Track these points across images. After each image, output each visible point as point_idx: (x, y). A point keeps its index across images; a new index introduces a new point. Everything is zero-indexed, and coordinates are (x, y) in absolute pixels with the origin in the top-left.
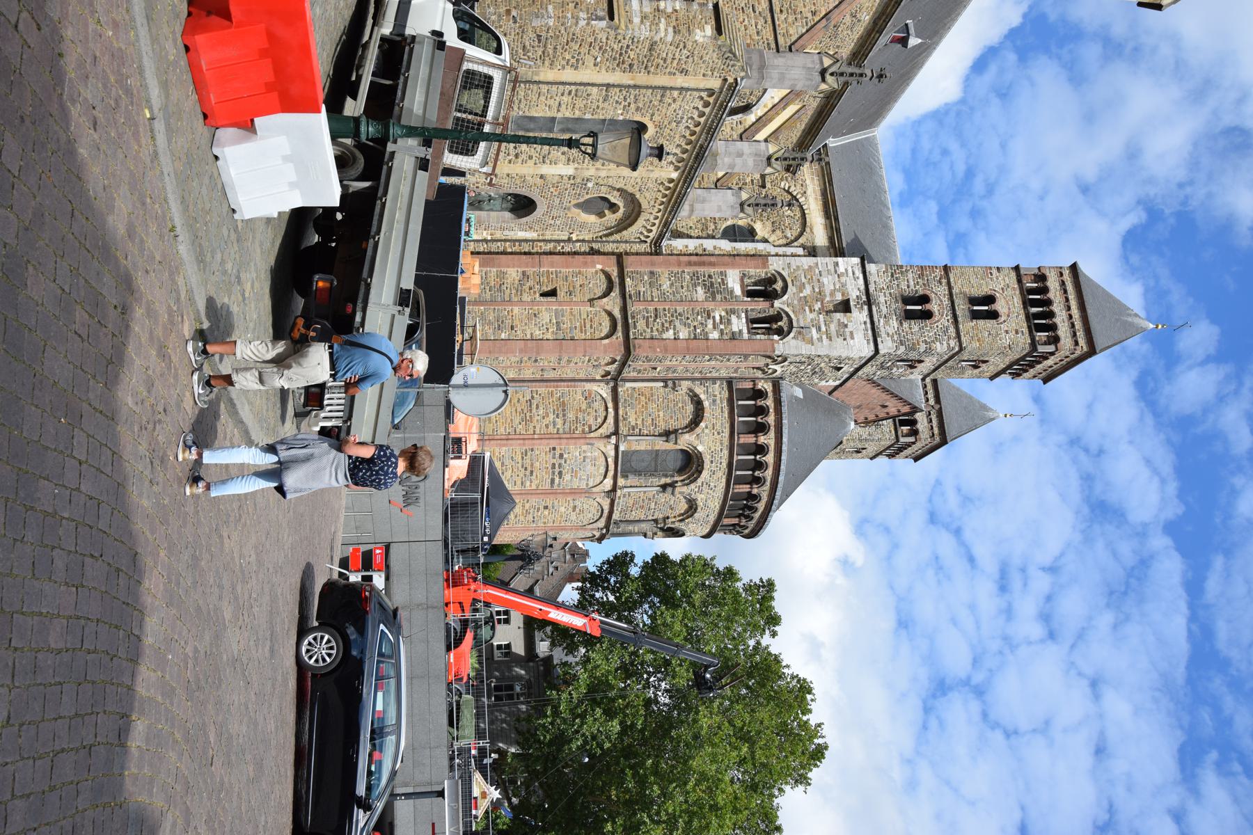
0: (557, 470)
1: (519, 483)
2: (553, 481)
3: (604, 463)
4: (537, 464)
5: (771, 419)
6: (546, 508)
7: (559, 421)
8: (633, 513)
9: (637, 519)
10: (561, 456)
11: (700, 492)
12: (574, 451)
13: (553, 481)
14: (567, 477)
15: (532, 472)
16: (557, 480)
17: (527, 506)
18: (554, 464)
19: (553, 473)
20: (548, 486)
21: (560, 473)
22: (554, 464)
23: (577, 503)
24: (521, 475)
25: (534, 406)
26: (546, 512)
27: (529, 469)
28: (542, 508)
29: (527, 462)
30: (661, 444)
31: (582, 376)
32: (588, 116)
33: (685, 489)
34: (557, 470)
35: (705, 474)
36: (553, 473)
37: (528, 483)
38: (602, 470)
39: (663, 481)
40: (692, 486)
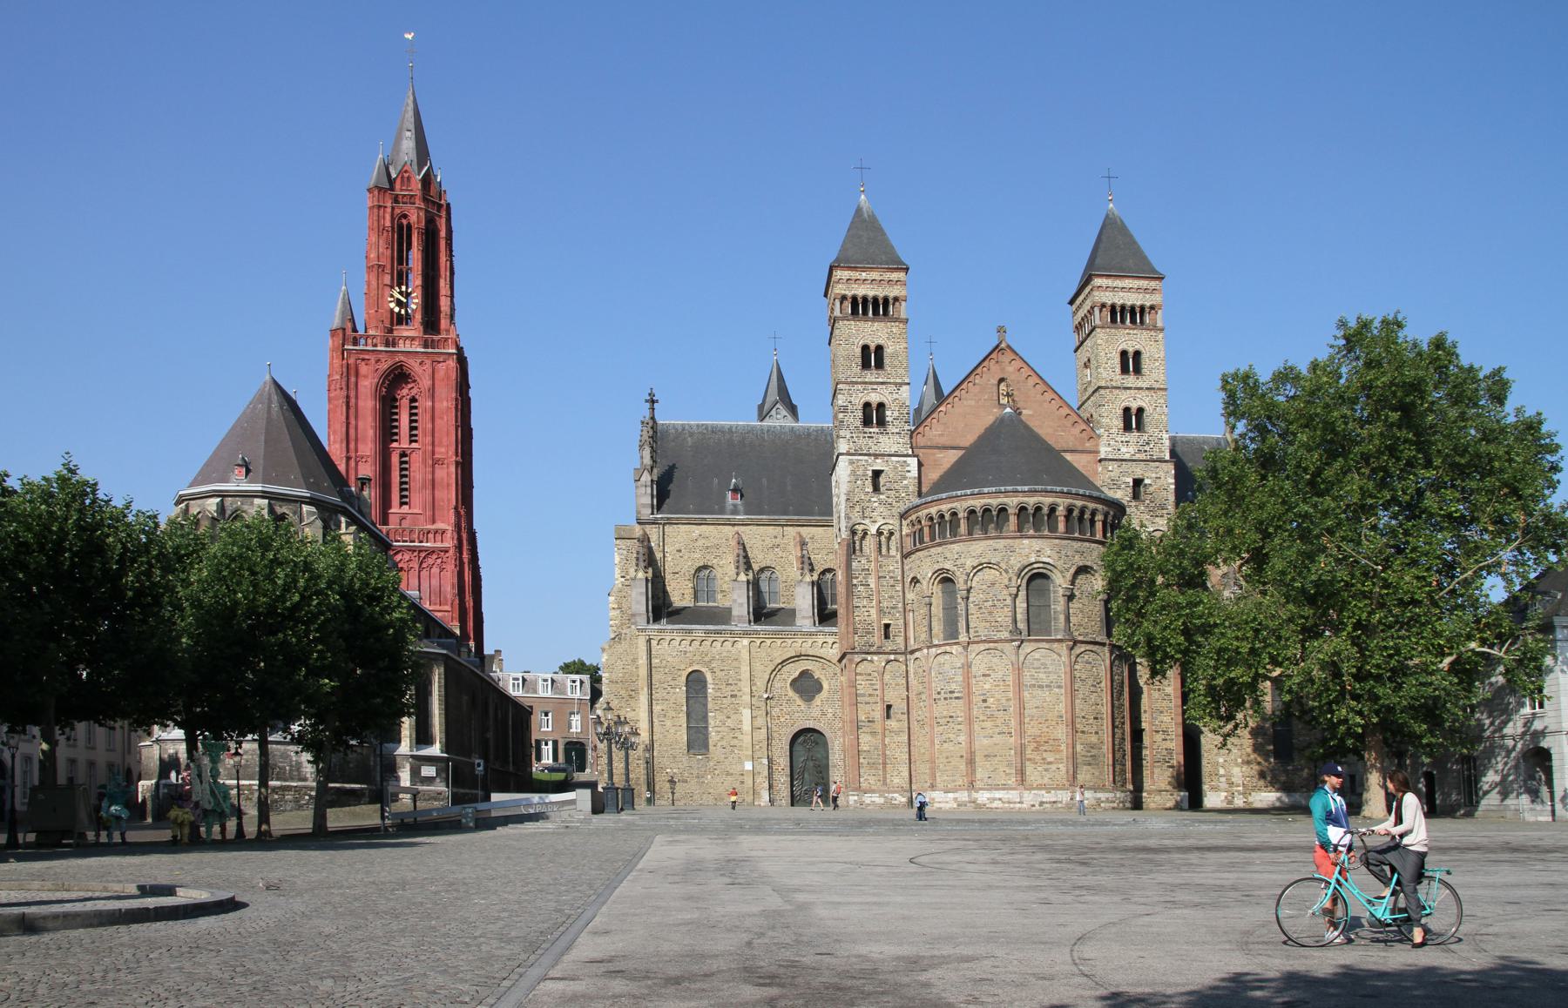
0: (948, 695)
1: (959, 727)
2: (957, 698)
3: (942, 656)
4: (945, 713)
5: (914, 517)
6: (985, 701)
7: (923, 697)
8: (999, 619)
9: (1010, 614)
10: (939, 693)
11: (963, 565)
12: (937, 685)
13: (957, 698)
14: (953, 687)
15: (951, 717)
16: (956, 695)
17: (982, 718)
18: (945, 699)
19: (951, 698)
20: (961, 701)
21: (951, 692)
22: (945, 699)
23: (980, 673)
24: (953, 725)
25: (919, 718)
26: (991, 700)
27: (948, 719)
28: (985, 705)
29: (943, 721)
30: (937, 610)
31: (904, 682)
32: (685, 708)
33: (961, 580)
34: (948, 695)
35: (947, 566)
36: (951, 698)
37: (960, 719)
38: (947, 657)
39: (960, 600)
40: (958, 574)
